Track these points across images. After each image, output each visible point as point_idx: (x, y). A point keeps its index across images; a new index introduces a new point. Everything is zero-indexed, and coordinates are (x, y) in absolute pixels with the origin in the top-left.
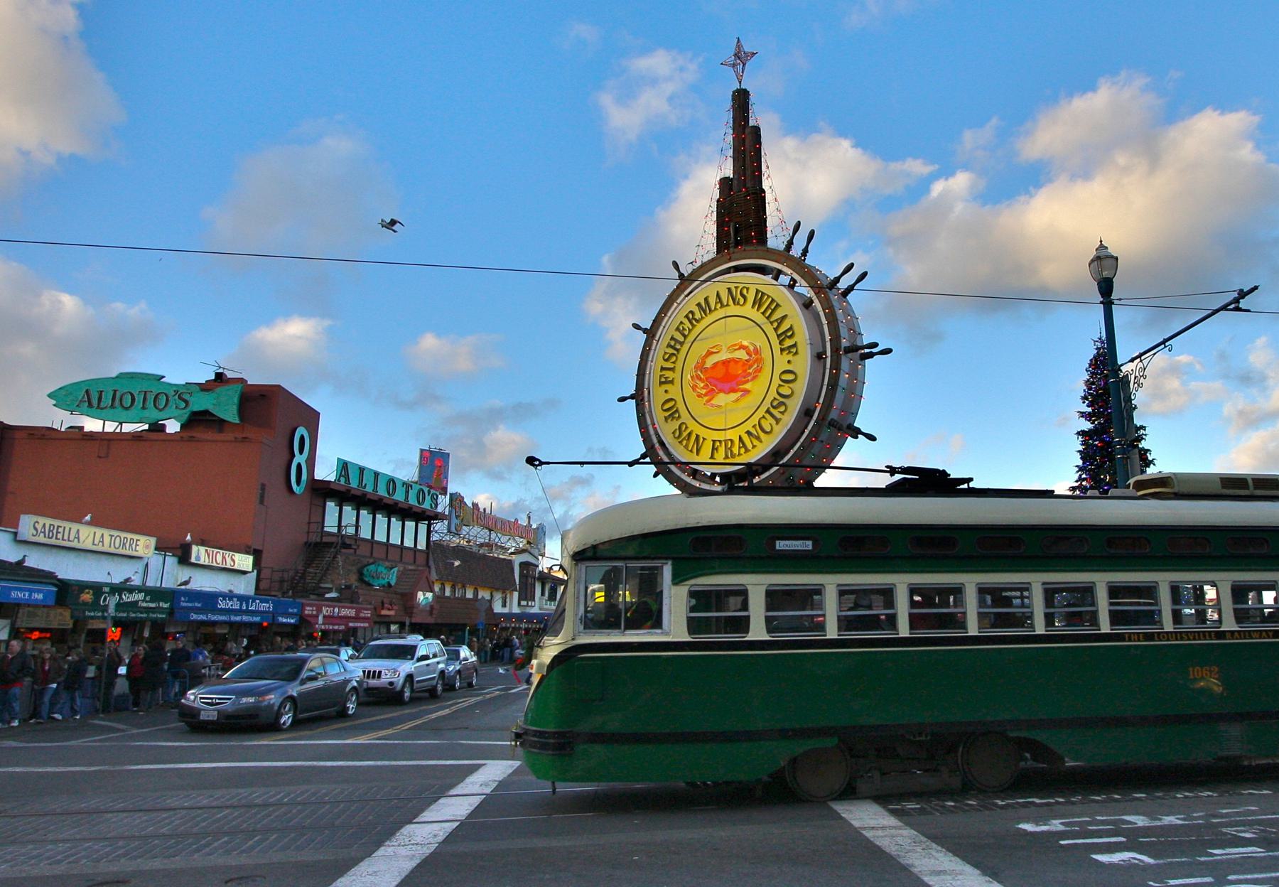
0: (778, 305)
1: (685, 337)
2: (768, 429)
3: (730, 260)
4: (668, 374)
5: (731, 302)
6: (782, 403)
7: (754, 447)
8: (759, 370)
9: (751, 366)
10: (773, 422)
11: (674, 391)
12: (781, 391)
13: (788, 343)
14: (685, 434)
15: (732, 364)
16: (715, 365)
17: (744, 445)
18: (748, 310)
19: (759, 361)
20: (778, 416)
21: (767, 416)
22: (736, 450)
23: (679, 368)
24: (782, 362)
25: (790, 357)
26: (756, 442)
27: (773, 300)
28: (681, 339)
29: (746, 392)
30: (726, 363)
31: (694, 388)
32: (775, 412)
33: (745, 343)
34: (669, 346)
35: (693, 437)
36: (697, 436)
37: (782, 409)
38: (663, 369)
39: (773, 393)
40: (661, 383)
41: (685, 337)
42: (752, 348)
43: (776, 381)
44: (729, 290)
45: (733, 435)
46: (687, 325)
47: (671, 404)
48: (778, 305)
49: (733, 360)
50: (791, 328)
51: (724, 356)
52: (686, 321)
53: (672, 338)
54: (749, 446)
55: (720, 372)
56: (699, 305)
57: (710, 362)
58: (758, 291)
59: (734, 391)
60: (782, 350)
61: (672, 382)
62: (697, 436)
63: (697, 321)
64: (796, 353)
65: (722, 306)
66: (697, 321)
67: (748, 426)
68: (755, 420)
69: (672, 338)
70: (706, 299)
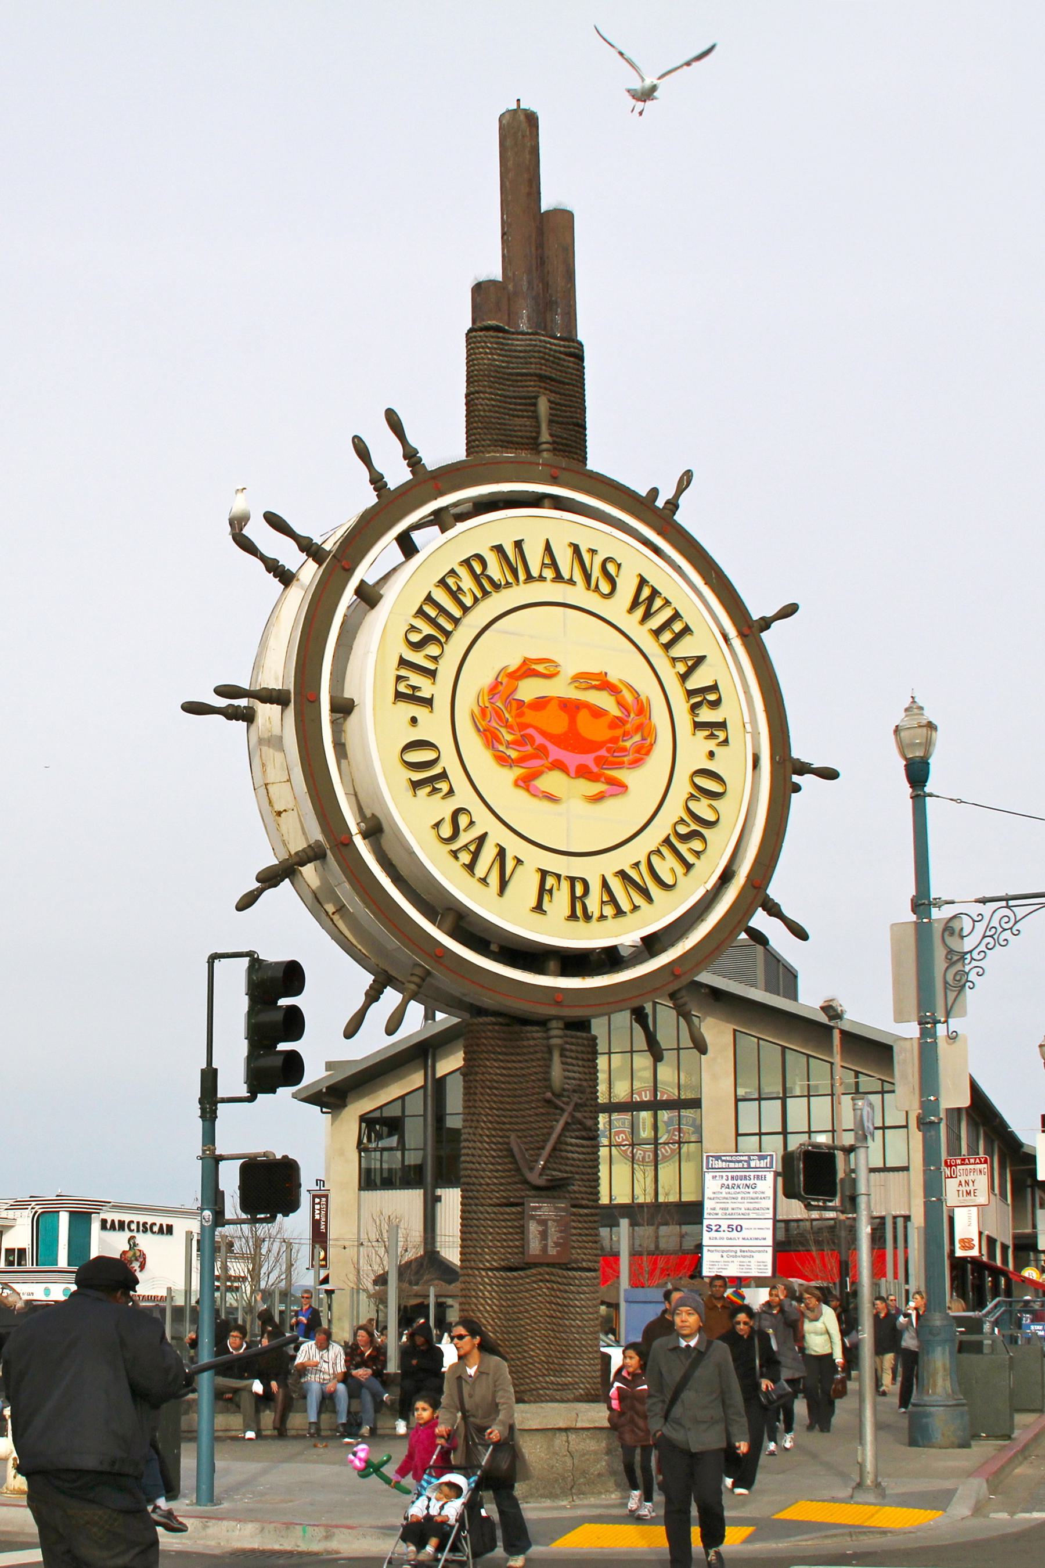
0: (687, 630)
1: (466, 610)
2: (670, 882)
3: (554, 481)
4: (416, 679)
5: (578, 576)
6: (694, 835)
7: (636, 908)
8: (643, 752)
9: (627, 735)
10: (680, 870)
11: (433, 726)
12: (692, 805)
13: (706, 715)
14: (464, 838)
15: (583, 716)
16: (540, 704)
17: (613, 901)
18: (617, 608)
19: (646, 729)
20: (690, 858)
21: (665, 850)
22: (593, 903)
23: (446, 670)
24: (695, 749)
25: (711, 745)
26: (638, 900)
27: (676, 616)
28: (457, 612)
29: (620, 787)
30: (571, 708)
31: (490, 738)
32: (682, 848)
33: (612, 678)
34: (421, 613)
35: (489, 853)
36: (502, 853)
37: (697, 845)
38: (403, 662)
39: (674, 810)
40: (399, 696)
41: (466, 610)
42: (629, 697)
43: (682, 788)
44: (576, 549)
45: (592, 870)
46: (467, 583)
47: (427, 755)
48: (687, 630)
49: (587, 706)
50: (714, 688)
51: (559, 688)
52: (463, 572)
53: (429, 599)
54: (625, 906)
55: (558, 723)
56: (499, 549)
57: (529, 690)
58: (643, 582)
59: (593, 777)
60: (698, 726)
61: (428, 702)
62: (502, 853)
63: (497, 587)
64: (726, 742)
65: (558, 577)
66: (497, 587)
67: (623, 859)
68: (638, 850)
69: (429, 599)
70: (518, 544)
